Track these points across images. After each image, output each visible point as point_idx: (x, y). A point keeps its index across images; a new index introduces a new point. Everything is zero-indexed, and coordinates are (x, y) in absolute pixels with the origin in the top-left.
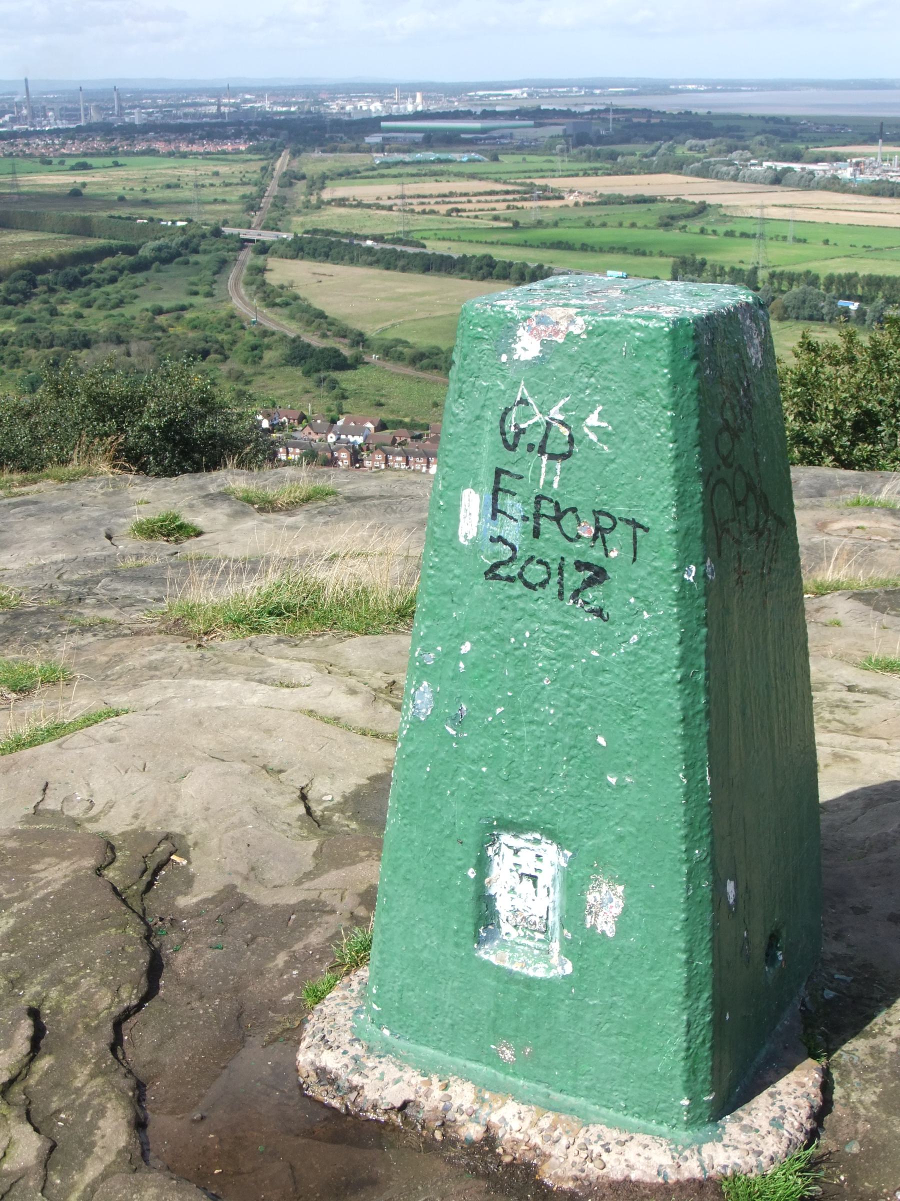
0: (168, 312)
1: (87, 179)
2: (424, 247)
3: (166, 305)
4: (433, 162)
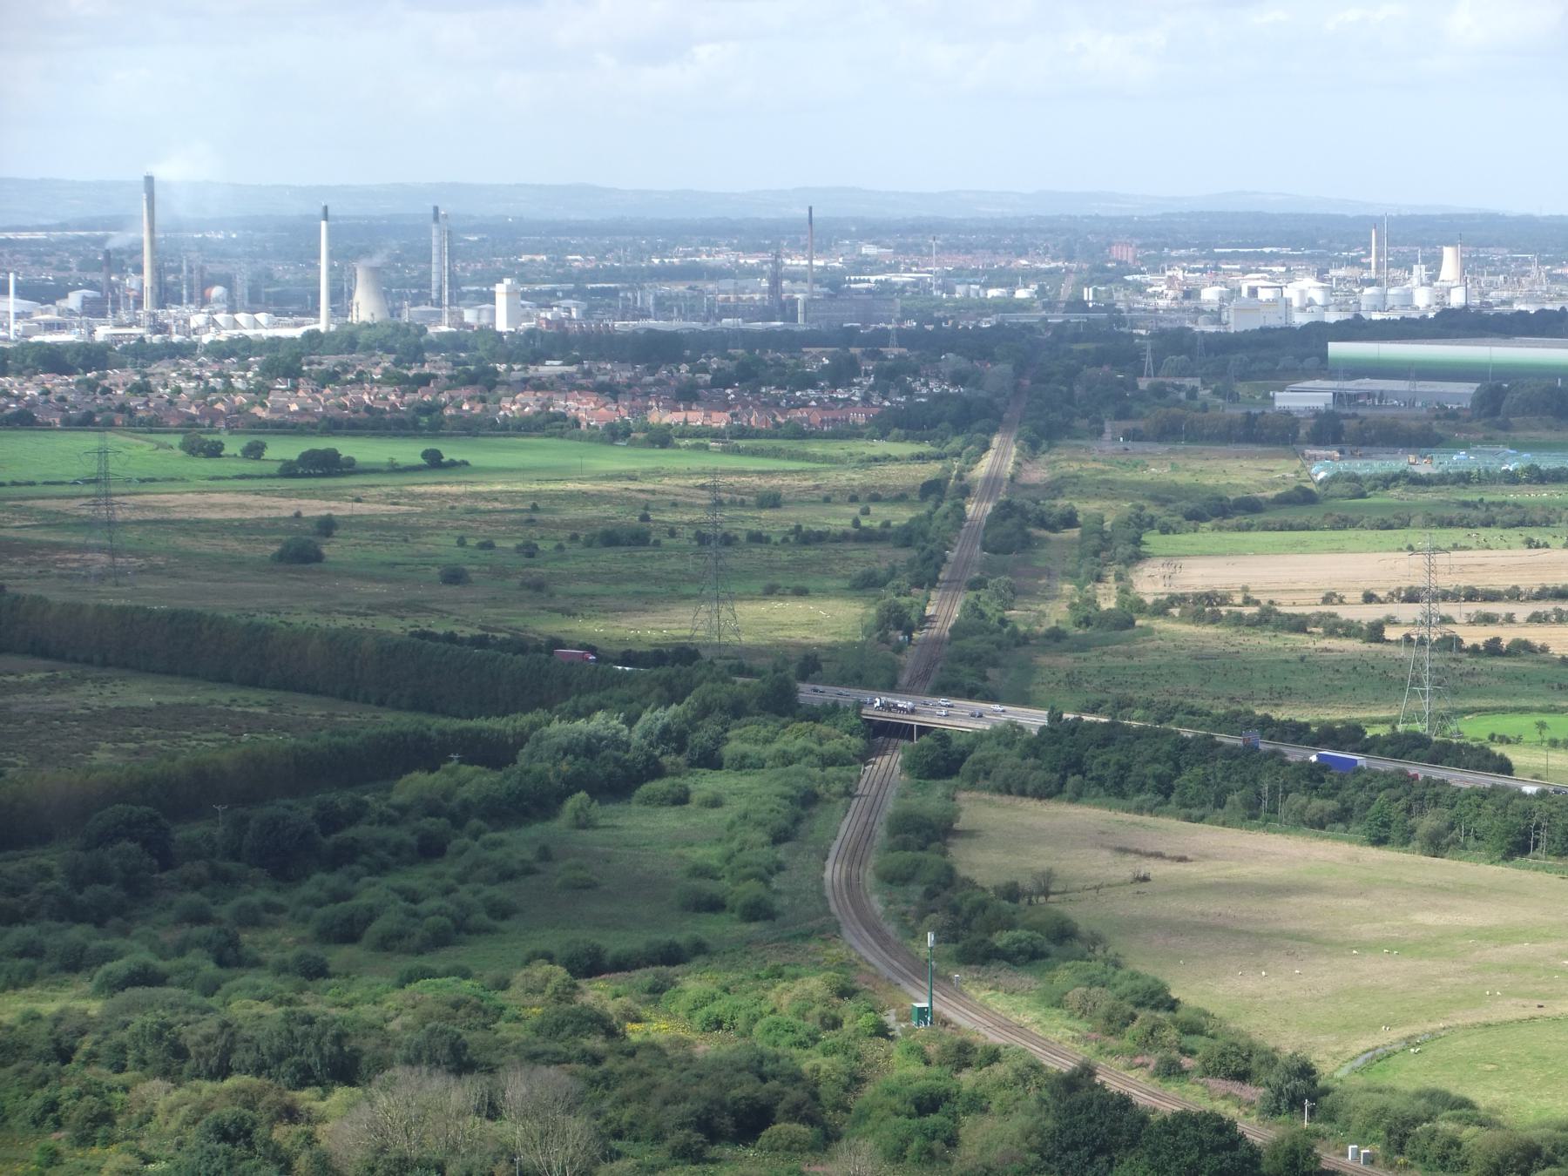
0: (622, 965)
1: (342, 509)
2: (1505, 767)
3: (614, 944)
4: (1512, 479)
